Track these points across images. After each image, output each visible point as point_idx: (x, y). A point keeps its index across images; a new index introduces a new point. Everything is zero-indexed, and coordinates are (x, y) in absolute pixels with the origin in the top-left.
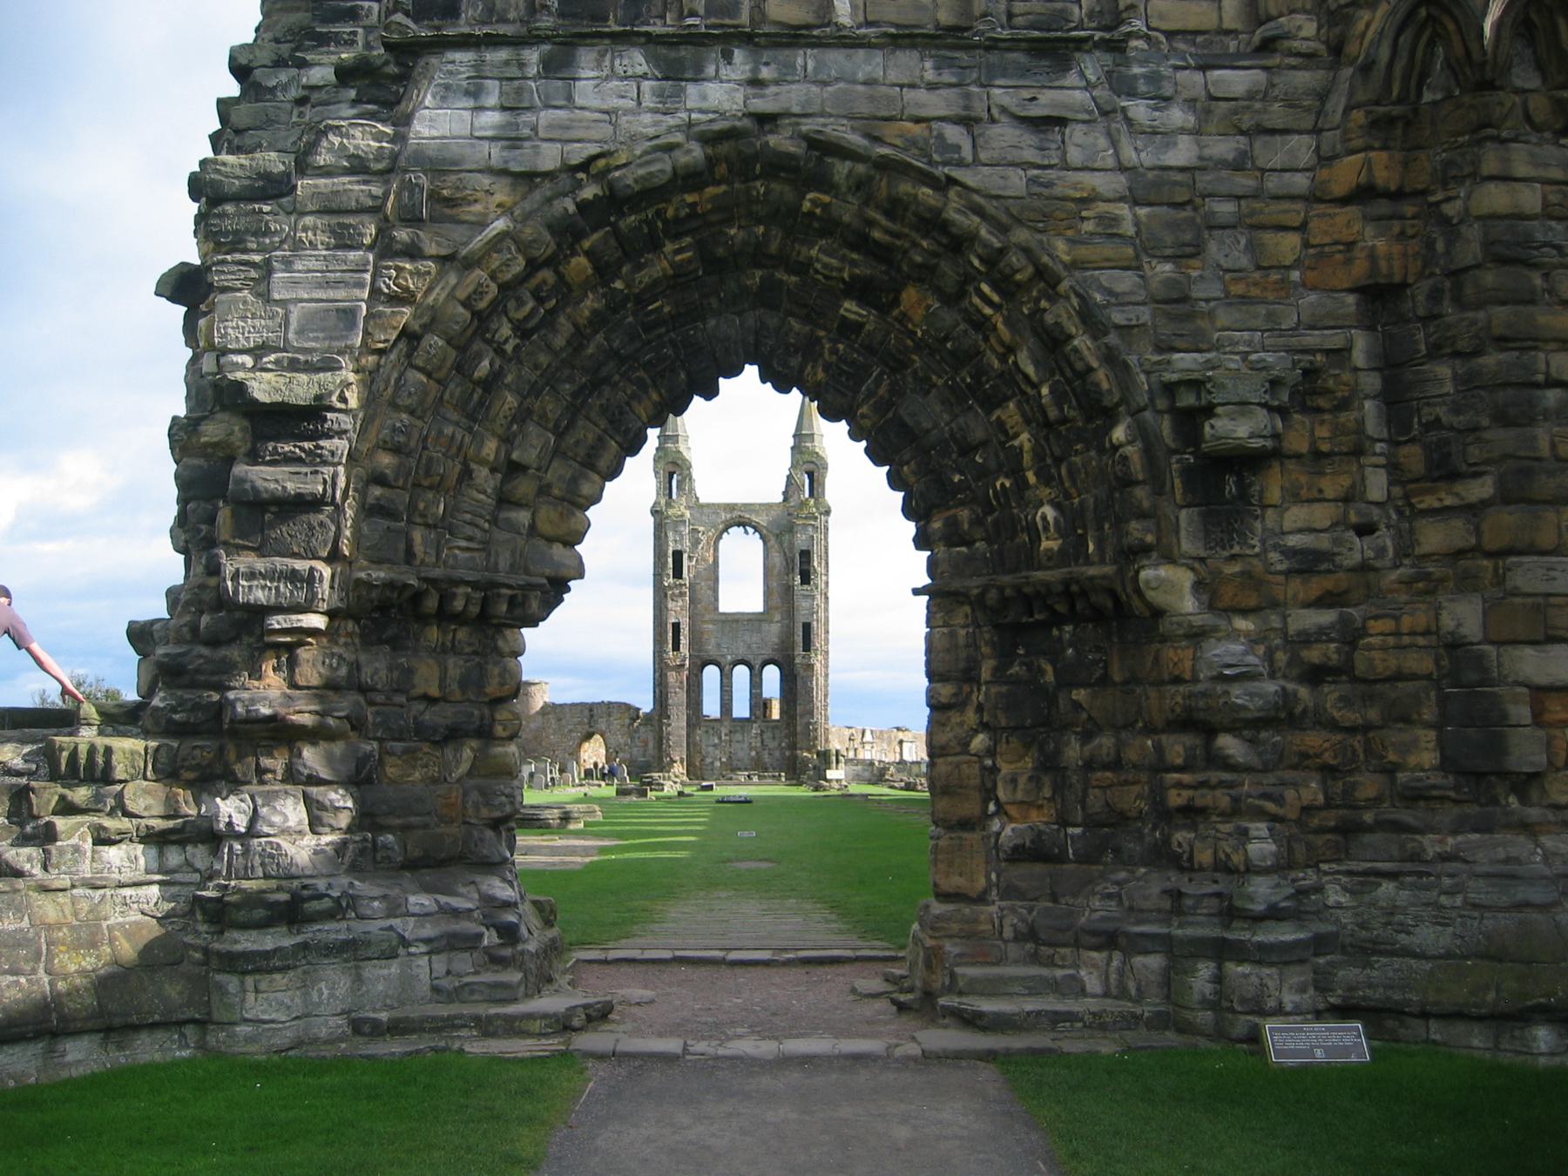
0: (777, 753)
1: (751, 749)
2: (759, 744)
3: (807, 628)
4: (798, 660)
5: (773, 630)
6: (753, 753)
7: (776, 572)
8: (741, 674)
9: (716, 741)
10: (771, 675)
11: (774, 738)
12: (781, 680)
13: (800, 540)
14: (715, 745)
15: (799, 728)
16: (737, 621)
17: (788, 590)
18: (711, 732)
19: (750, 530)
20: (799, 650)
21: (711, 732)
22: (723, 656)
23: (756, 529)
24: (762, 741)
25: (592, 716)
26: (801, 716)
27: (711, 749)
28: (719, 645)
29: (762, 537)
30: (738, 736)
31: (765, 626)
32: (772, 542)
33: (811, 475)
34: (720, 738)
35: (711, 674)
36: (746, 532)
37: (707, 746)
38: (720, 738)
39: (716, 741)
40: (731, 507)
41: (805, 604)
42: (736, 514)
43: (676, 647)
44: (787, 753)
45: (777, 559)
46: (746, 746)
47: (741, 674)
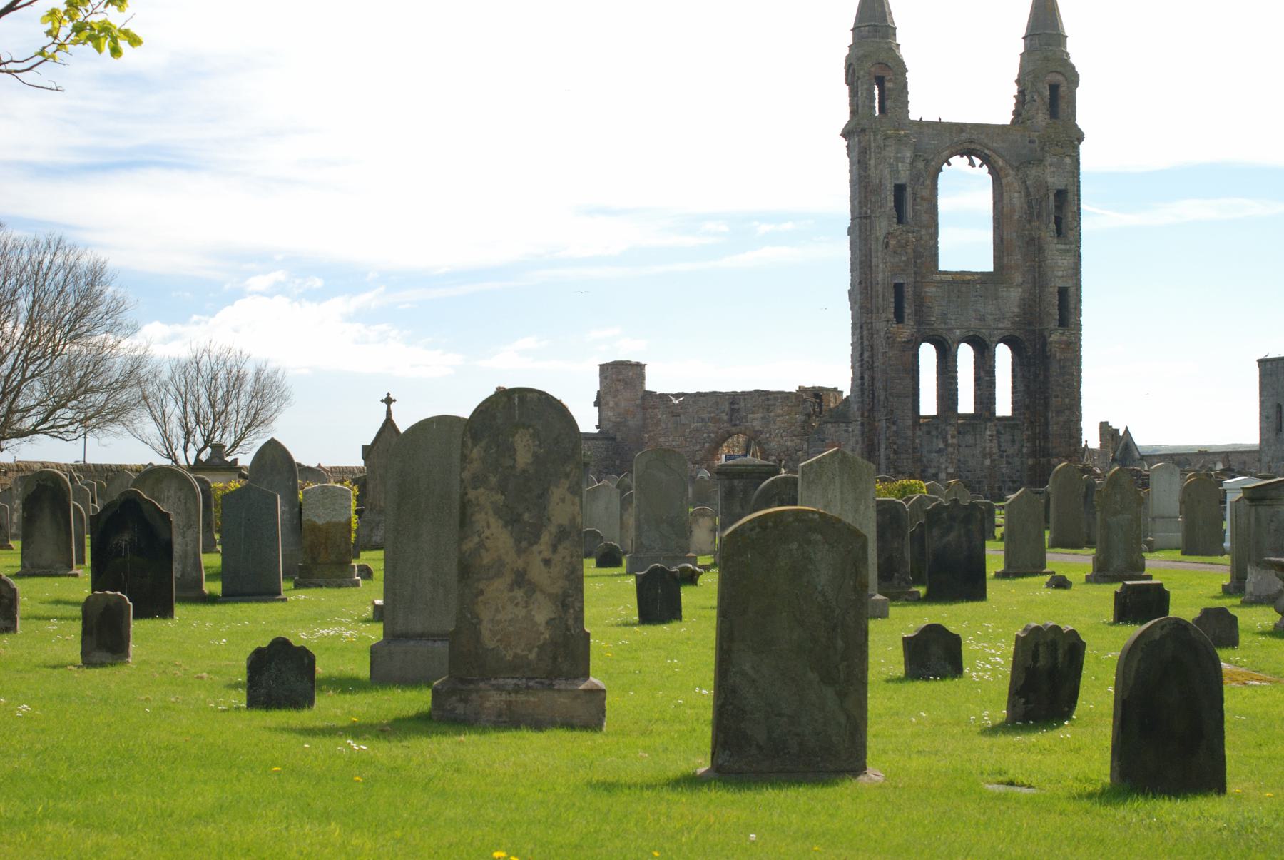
0: (1017, 461)
1: (984, 456)
2: (995, 450)
3: (1063, 292)
4: (1055, 337)
5: (1013, 297)
6: (988, 462)
7: (1016, 217)
8: (965, 355)
9: (942, 446)
10: (1003, 356)
11: (1013, 442)
12: (1013, 364)
13: (1055, 181)
14: (939, 451)
15: (1054, 429)
16: (968, 282)
17: (1034, 247)
18: (934, 433)
19: (977, 161)
20: (1053, 322)
21: (934, 433)
22: (950, 330)
23: (986, 160)
24: (1000, 446)
25: (733, 411)
26: (1059, 413)
27: (934, 455)
28: (944, 315)
29: (992, 171)
30: (969, 439)
31: (1002, 290)
32: (1011, 178)
33: (1054, 88)
34: (945, 441)
35: (928, 355)
36: (972, 164)
37: (930, 452)
38: (945, 441)
39: (942, 446)
40: (961, 128)
41: (1065, 262)
42: (964, 136)
43: (899, 317)
44: (1030, 462)
45: (1016, 200)
46: (978, 451)
47: (965, 355)
